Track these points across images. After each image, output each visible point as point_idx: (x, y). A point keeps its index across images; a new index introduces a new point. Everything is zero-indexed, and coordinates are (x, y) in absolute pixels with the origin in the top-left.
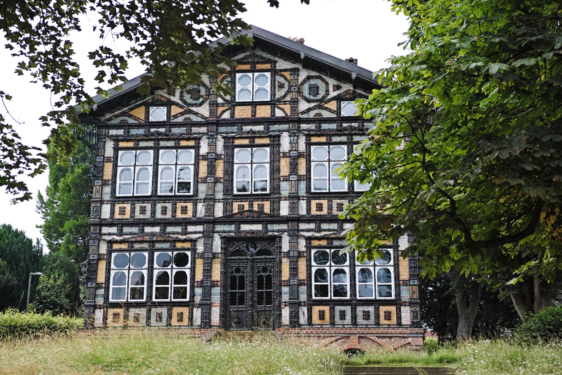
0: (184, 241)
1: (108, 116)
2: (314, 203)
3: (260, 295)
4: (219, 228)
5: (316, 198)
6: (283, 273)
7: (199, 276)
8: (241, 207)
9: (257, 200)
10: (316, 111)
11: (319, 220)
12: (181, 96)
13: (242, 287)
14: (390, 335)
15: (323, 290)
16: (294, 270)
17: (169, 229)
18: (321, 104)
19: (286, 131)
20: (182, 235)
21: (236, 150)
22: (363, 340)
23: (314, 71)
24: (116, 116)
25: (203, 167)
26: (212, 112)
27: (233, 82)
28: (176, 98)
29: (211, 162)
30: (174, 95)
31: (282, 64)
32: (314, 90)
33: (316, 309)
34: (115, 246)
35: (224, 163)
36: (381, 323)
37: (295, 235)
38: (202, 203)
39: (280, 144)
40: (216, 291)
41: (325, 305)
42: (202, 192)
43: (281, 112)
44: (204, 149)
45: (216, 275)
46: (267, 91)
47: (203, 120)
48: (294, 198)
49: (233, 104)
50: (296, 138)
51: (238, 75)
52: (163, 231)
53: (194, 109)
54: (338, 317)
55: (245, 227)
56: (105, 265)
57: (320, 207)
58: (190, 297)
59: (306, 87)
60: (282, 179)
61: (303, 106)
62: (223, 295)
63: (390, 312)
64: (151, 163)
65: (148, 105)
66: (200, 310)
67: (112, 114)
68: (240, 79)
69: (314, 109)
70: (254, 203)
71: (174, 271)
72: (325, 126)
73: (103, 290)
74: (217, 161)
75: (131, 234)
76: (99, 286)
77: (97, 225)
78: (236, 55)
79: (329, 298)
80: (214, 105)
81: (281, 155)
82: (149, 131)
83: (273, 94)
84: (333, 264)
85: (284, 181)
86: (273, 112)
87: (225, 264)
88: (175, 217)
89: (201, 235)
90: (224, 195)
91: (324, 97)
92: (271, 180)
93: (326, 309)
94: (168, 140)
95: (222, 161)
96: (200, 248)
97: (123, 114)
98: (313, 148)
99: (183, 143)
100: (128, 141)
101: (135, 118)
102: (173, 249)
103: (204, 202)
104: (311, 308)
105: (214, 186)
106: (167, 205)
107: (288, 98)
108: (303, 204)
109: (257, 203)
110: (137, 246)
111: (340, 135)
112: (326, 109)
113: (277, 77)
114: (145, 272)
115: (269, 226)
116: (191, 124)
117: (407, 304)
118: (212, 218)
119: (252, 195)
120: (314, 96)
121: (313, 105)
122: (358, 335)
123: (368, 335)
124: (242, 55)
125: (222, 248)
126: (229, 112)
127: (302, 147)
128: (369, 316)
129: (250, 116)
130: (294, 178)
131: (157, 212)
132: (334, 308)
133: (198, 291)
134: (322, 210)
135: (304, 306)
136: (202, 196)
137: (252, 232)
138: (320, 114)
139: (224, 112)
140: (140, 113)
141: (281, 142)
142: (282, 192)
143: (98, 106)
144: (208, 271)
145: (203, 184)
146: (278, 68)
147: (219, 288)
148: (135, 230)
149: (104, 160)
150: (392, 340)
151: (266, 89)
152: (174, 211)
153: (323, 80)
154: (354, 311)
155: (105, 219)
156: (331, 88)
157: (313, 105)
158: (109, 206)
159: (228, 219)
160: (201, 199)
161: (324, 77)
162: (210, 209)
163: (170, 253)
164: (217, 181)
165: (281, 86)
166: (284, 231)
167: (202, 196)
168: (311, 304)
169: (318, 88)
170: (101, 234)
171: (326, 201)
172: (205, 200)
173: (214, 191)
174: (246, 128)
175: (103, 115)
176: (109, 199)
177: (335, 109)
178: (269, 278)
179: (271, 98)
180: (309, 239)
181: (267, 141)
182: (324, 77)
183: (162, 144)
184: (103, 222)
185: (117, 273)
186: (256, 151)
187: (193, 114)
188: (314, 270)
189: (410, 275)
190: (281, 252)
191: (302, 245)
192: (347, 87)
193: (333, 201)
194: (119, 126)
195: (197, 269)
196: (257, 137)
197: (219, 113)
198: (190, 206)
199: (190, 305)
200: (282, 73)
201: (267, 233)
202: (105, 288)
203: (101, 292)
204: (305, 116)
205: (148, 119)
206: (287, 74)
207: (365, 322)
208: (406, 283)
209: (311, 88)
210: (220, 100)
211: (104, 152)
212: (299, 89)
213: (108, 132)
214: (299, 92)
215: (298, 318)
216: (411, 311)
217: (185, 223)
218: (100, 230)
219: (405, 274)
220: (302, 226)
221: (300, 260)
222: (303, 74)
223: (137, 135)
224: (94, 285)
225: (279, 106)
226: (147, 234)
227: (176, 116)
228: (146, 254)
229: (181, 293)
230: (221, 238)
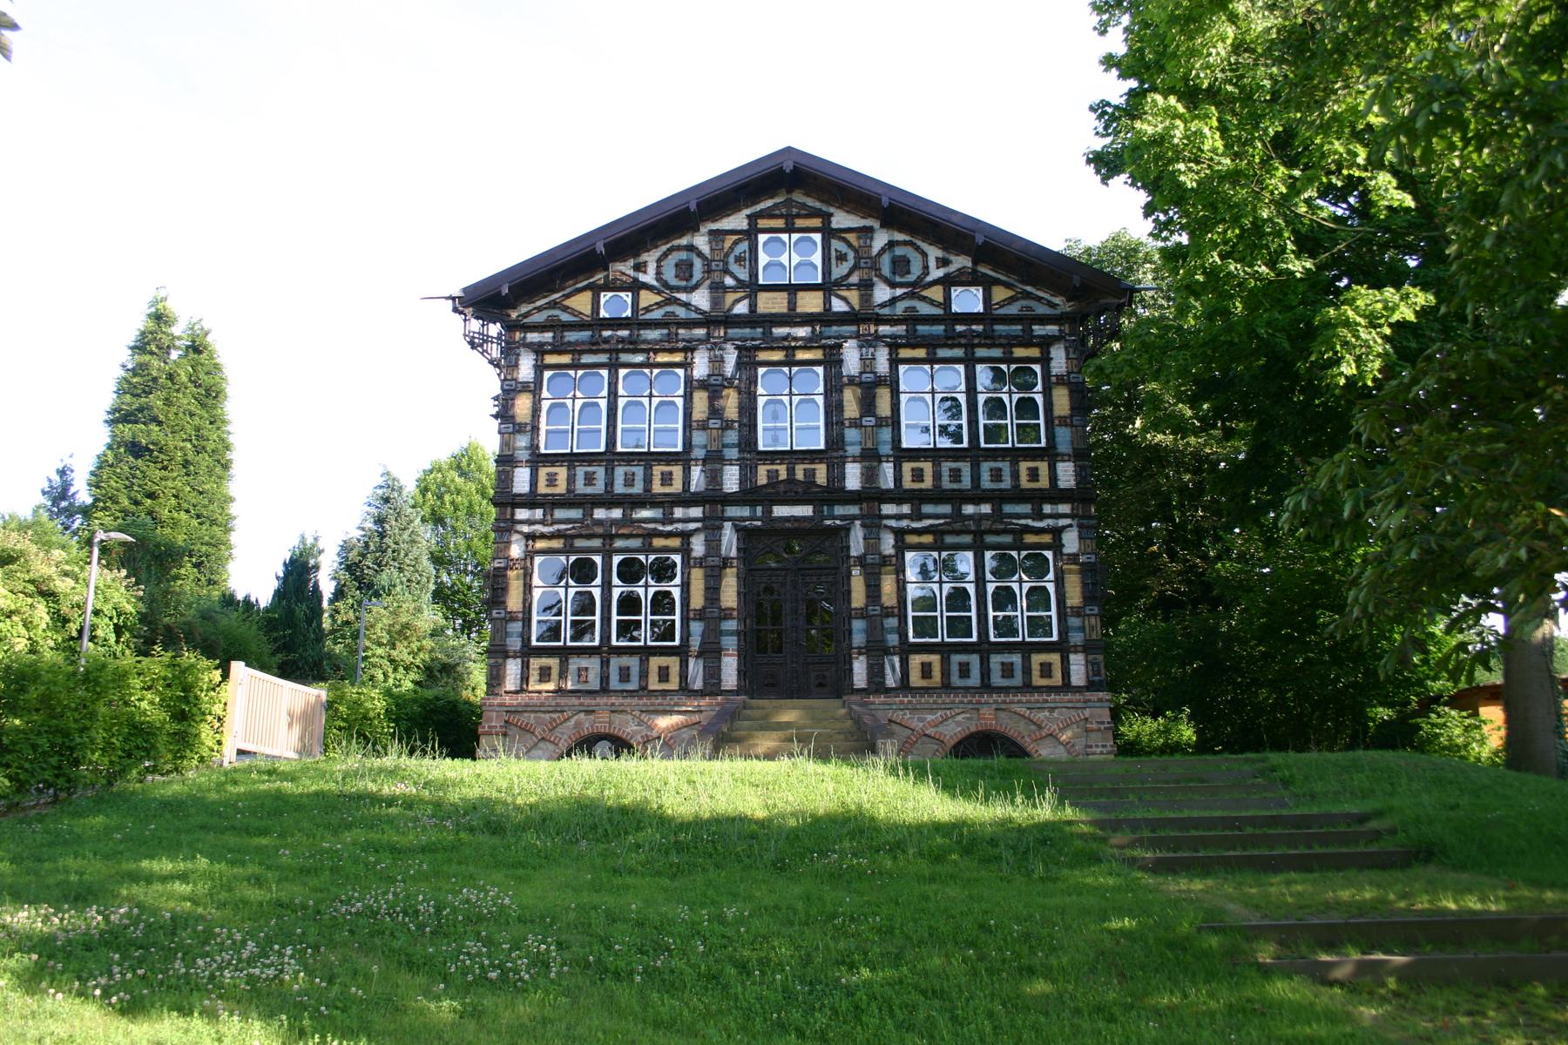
0: (669, 535)
1: (524, 309)
2: (907, 467)
4: (732, 511)
5: (911, 459)
6: (854, 595)
8: (772, 475)
9: (803, 461)
11: (917, 498)
12: (659, 273)
14: (1052, 705)
16: (873, 591)
18: (916, 289)
20: (664, 524)
21: (761, 371)
24: (539, 309)
25: (701, 400)
26: (715, 303)
27: (753, 250)
28: (648, 278)
30: (645, 272)
31: (841, 220)
32: (901, 265)
33: (916, 661)
37: (873, 524)
38: (699, 468)
39: (842, 361)
44: (701, 368)
45: (729, 595)
46: (815, 267)
48: (870, 457)
49: (752, 288)
50: (871, 350)
51: (762, 238)
53: (683, 296)
54: (957, 673)
55: (780, 511)
57: (918, 475)
58: (682, 638)
59: (886, 261)
61: (882, 293)
65: (596, 290)
66: (701, 662)
67: (531, 306)
68: (765, 244)
70: (797, 467)
71: (651, 591)
72: (923, 329)
73: (520, 624)
76: (511, 618)
79: (939, 640)
80: (718, 289)
83: (827, 272)
85: (850, 427)
86: (827, 302)
88: (650, 491)
89: (699, 525)
90: (740, 452)
91: (920, 279)
92: (826, 425)
93: (935, 659)
96: (698, 546)
97: (554, 305)
98: (902, 368)
100: (560, 352)
101: (573, 312)
102: (647, 549)
106: (634, 469)
107: (854, 279)
108: (888, 469)
111: (952, 347)
112: (924, 299)
117: (1080, 649)
121: (899, 292)
122: (994, 706)
123: (1012, 706)
124: (769, 203)
125: (738, 549)
126: (746, 302)
127: (882, 365)
128: (1012, 670)
129: (785, 311)
130: (869, 421)
131: (616, 482)
133: (696, 628)
134: (923, 481)
135: (895, 654)
136: (698, 453)
138: (913, 309)
139: (738, 301)
140: (581, 303)
142: (848, 448)
144: (713, 592)
145: (701, 433)
146: (834, 225)
148: (575, 514)
150: (1055, 715)
152: (648, 480)
153: (917, 248)
154: (985, 663)
155: (520, 495)
156: (932, 263)
157: (899, 292)
160: (697, 460)
161: (919, 243)
162: (714, 477)
165: (842, 258)
166: (853, 518)
167: (698, 453)
168: (906, 650)
169: (909, 262)
171: (930, 464)
172: (705, 461)
174: (779, 331)
177: (941, 300)
181: (817, 355)
182: (919, 243)
183: (624, 358)
184: (518, 500)
186: (797, 372)
187: (680, 305)
190: (849, 557)
191: (888, 544)
192: (960, 262)
193: (943, 464)
196: (800, 348)
198: (677, 471)
199: (682, 652)
203: (516, 627)
204: (886, 311)
205: (598, 314)
206: (851, 237)
208: (1078, 612)
210: (729, 281)
215: (883, 676)
218: (513, 514)
219: (1074, 598)
220: (888, 509)
222: (880, 240)
223: (577, 343)
224: (503, 615)
225: (839, 293)
226: (600, 522)
227: (648, 310)
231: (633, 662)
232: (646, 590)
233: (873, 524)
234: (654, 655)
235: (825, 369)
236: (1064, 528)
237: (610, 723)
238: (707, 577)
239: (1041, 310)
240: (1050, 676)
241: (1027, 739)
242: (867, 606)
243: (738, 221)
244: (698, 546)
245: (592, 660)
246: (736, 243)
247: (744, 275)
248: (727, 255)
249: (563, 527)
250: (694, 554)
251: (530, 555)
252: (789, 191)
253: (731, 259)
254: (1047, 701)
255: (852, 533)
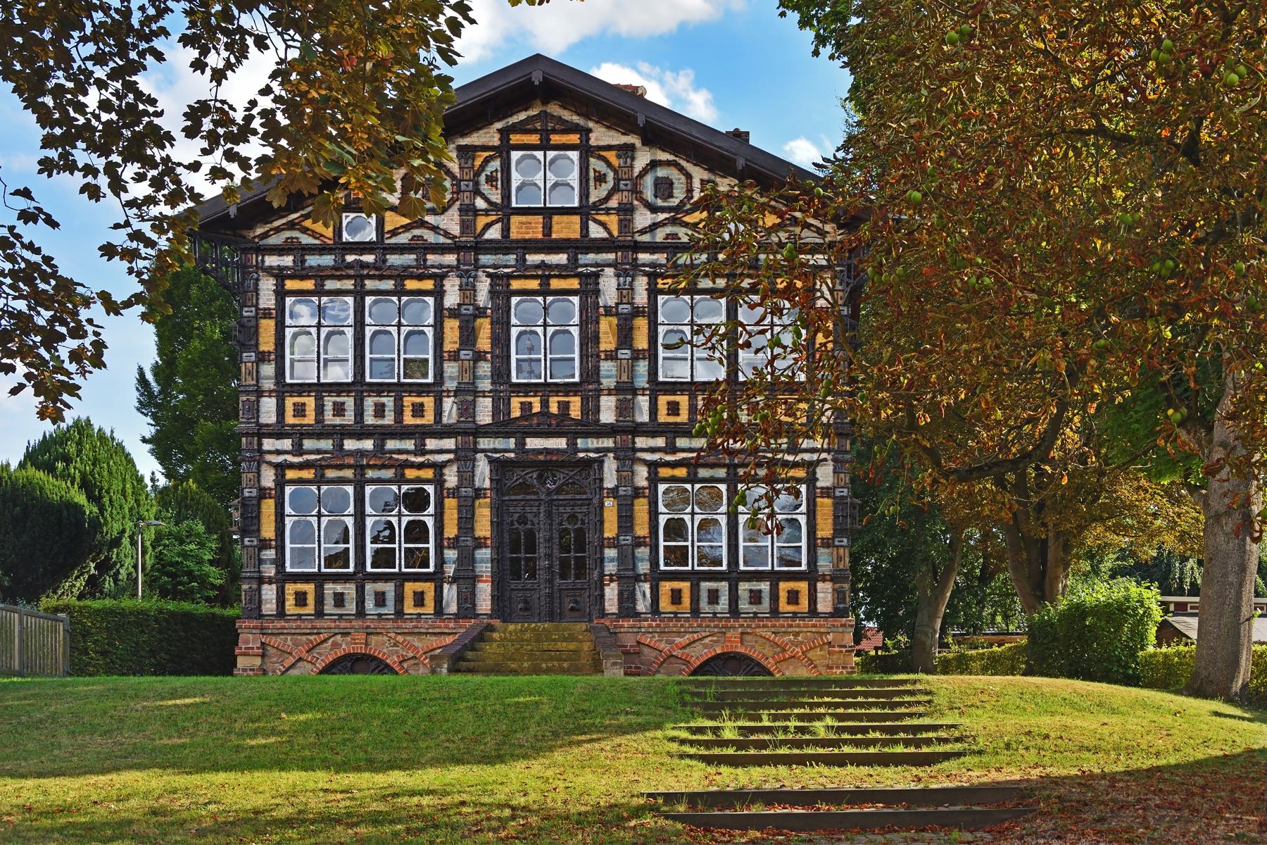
0: (420, 466)
1: (259, 231)
3: (564, 564)
4: (484, 443)
5: (666, 393)
6: (606, 525)
7: (451, 531)
8: (526, 407)
10: (669, 230)
13: (532, 548)
15: (678, 555)
16: (626, 521)
17: (391, 444)
19: (609, 265)
21: (514, 300)
22: (748, 638)
23: (663, 151)
24: (278, 230)
25: (452, 328)
26: (466, 227)
29: (468, 321)
31: (601, 136)
32: (664, 188)
33: (666, 587)
34: (290, 474)
35: (492, 324)
36: (781, 609)
37: (627, 457)
38: (452, 399)
40: (484, 554)
41: (683, 580)
42: (451, 378)
43: (601, 229)
44: (452, 298)
45: (483, 527)
47: (449, 241)
48: (626, 390)
49: (505, 211)
50: (629, 279)
51: (515, 155)
52: (380, 448)
53: (430, 219)
55: (533, 443)
56: (273, 507)
59: (649, 180)
60: (603, 356)
62: (496, 561)
63: (797, 592)
64: (351, 321)
66: (455, 587)
68: (519, 162)
69: (664, 225)
71: (405, 520)
73: (273, 552)
74: (479, 321)
75: (318, 452)
76: (264, 544)
77: (253, 435)
78: (511, 115)
79: (689, 568)
80: (469, 212)
81: (602, 310)
82: (344, 260)
83: (584, 194)
84: (697, 510)
85: (606, 359)
86: (585, 228)
87: (499, 511)
89: (451, 456)
90: (492, 384)
93: (685, 586)
94: (381, 278)
95: (488, 320)
96: (451, 479)
97: (291, 226)
99: (411, 285)
100: (303, 278)
102: (400, 480)
103: (455, 396)
104: (657, 586)
105: (474, 367)
106: (384, 400)
107: (613, 203)
108: (643, 402)
109: (556, 399)
110: (331, 474)
113: (592, 160)
114: (350, 522)
115: (579, 441)
116: (425, 248)
118: (471, 425)
119: (546, 384)
120: (665, 200)
121: (661, 217)
122: (740, 630)
124: (522, 116)
125: (491, 480)
126: (499, 226)
127: (641, 298)
129: (540, 236)
130: (625, 354)
132: (698, 585)
133: (451, 554)
134: (678, 415)
135: (645, 581)
136: (450, 385)
137: (547, 451)
141: (601, 287)
143: (238, 209)
144: (466, 522)
145: (453, 364)
146: (593, 142)
147: (488, 551)
148: (326, 444)
149: (257, 313)
150: (800, 638)
151: (571, 183)
152: (399, 411)
153: (681, 169)
155: (268, 425)
157: (661, 217)
158: (274, 400)
159: (501, 427)
160: (449, 391)
161: (684, 163)
162: (467, 410)
163: (395, 488)
164: (479, 357)
165: (601, 178)
166: (608, 450)
167: (450, 385)
168: (656, 577)
169: (672, 184)
170: (261, 452)
171: (686, 398)
172: (457, 393)
173: (475, 377)
174: (533, 259)
175: (251, 227)
176: (272, 387)
178: (580, 535)
179: (581, 201)
180: (653, 466)
181: (574, 284)
182: (684, 163)
184: (264, 430)
185: (299, 522)
187: (428, 228)
188: (662, 520)
189: (835, 530)
190: (602, 488)
194: (283, 249)
195: (446, 517)
196: (555, 276)
197: (479, 227)
200: (603, 153)
201: (575, 454)
202: (276, 548)
203: (270, 554)
204: (646, 238)
205: (340, 236)
206: (611, 156)
207: (754, 609)
208: (827, 543)
209: (658, 183)
210: (480, 203)
211: (257, 299)
212: (635, 185)
213: (263, 261)
214: (636, 191)
215: (634, 601)
216: (834, 590)
217: (421, 434)
218: (260, 444)
219: (825, 529)
220: (641, 442)
221: (637, 502)
222: (643, 159)
223: (320, 268)
225: (598, 217)
226: (351, 453)
227: (394, 233)
228: (350, 489)
230: (490, 462)
231: (389, 588)
233: (627, 457)
234: (409, 580)
235: (581, 299)
236: (819, 462)
237: (366, 644)
238: (460, 507)
239: (809, 237)
240: (797, 603)
241: (771, 660)
242: (618, 536)
243: (489, 136)
244: (451, 479)
245: (348, 585)
246: (487, 161)
247: (496, 197)
248: (477, 174)
249: (313, 457)
250: (448, 485)
251: (281, 483)
252: (545, 103)
253: (483, 178)
254: (791, 626)
255: (606, 465)
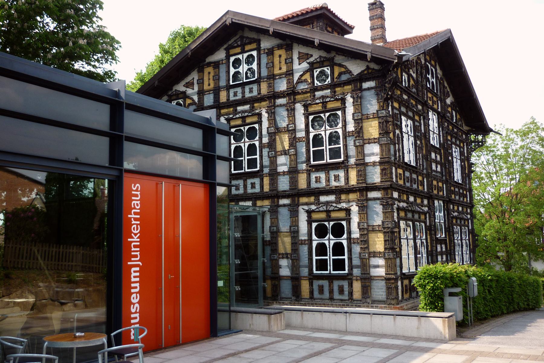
71: (332, 242)
229: (339, 265)
231: (325, 283)
232: (330, 241)
